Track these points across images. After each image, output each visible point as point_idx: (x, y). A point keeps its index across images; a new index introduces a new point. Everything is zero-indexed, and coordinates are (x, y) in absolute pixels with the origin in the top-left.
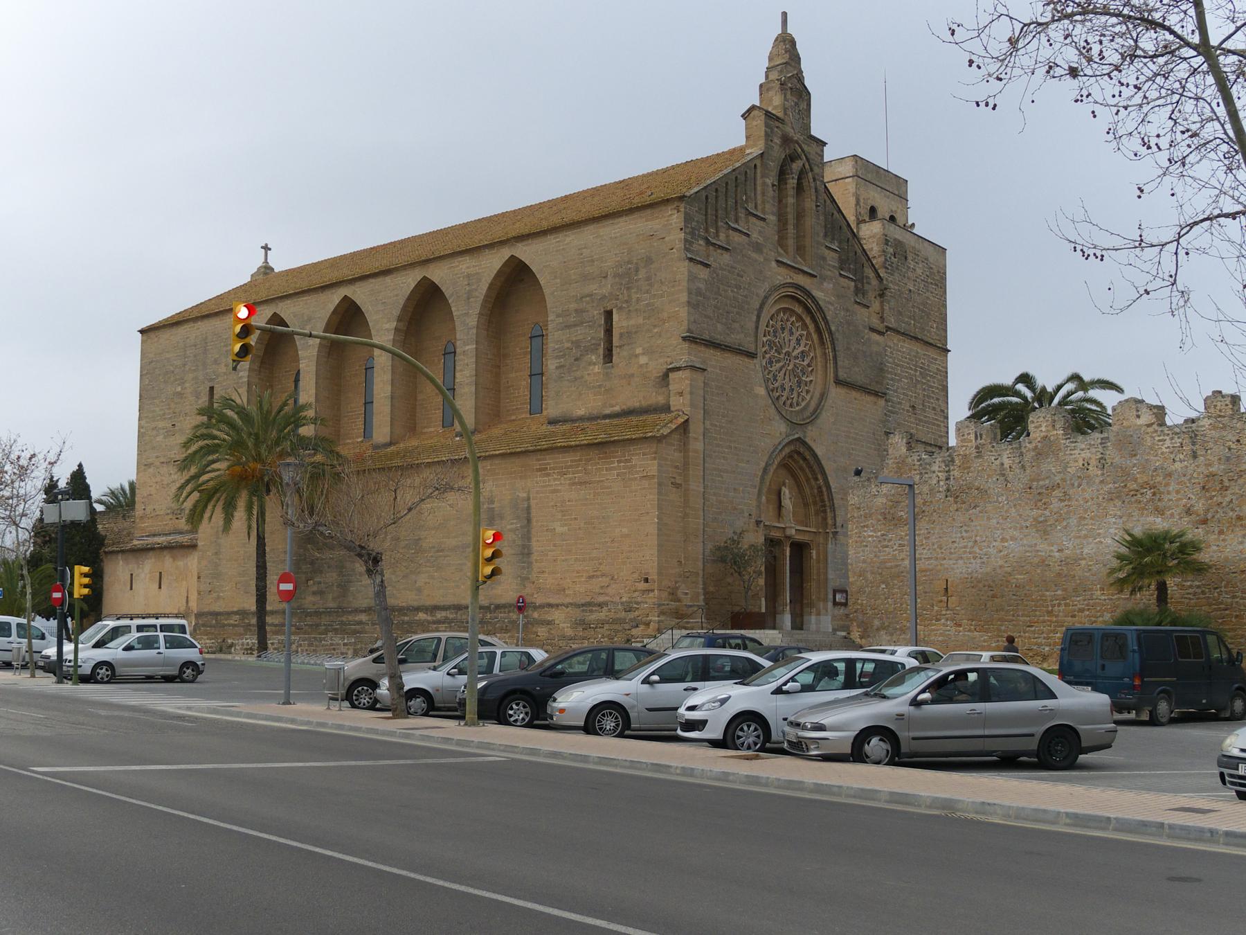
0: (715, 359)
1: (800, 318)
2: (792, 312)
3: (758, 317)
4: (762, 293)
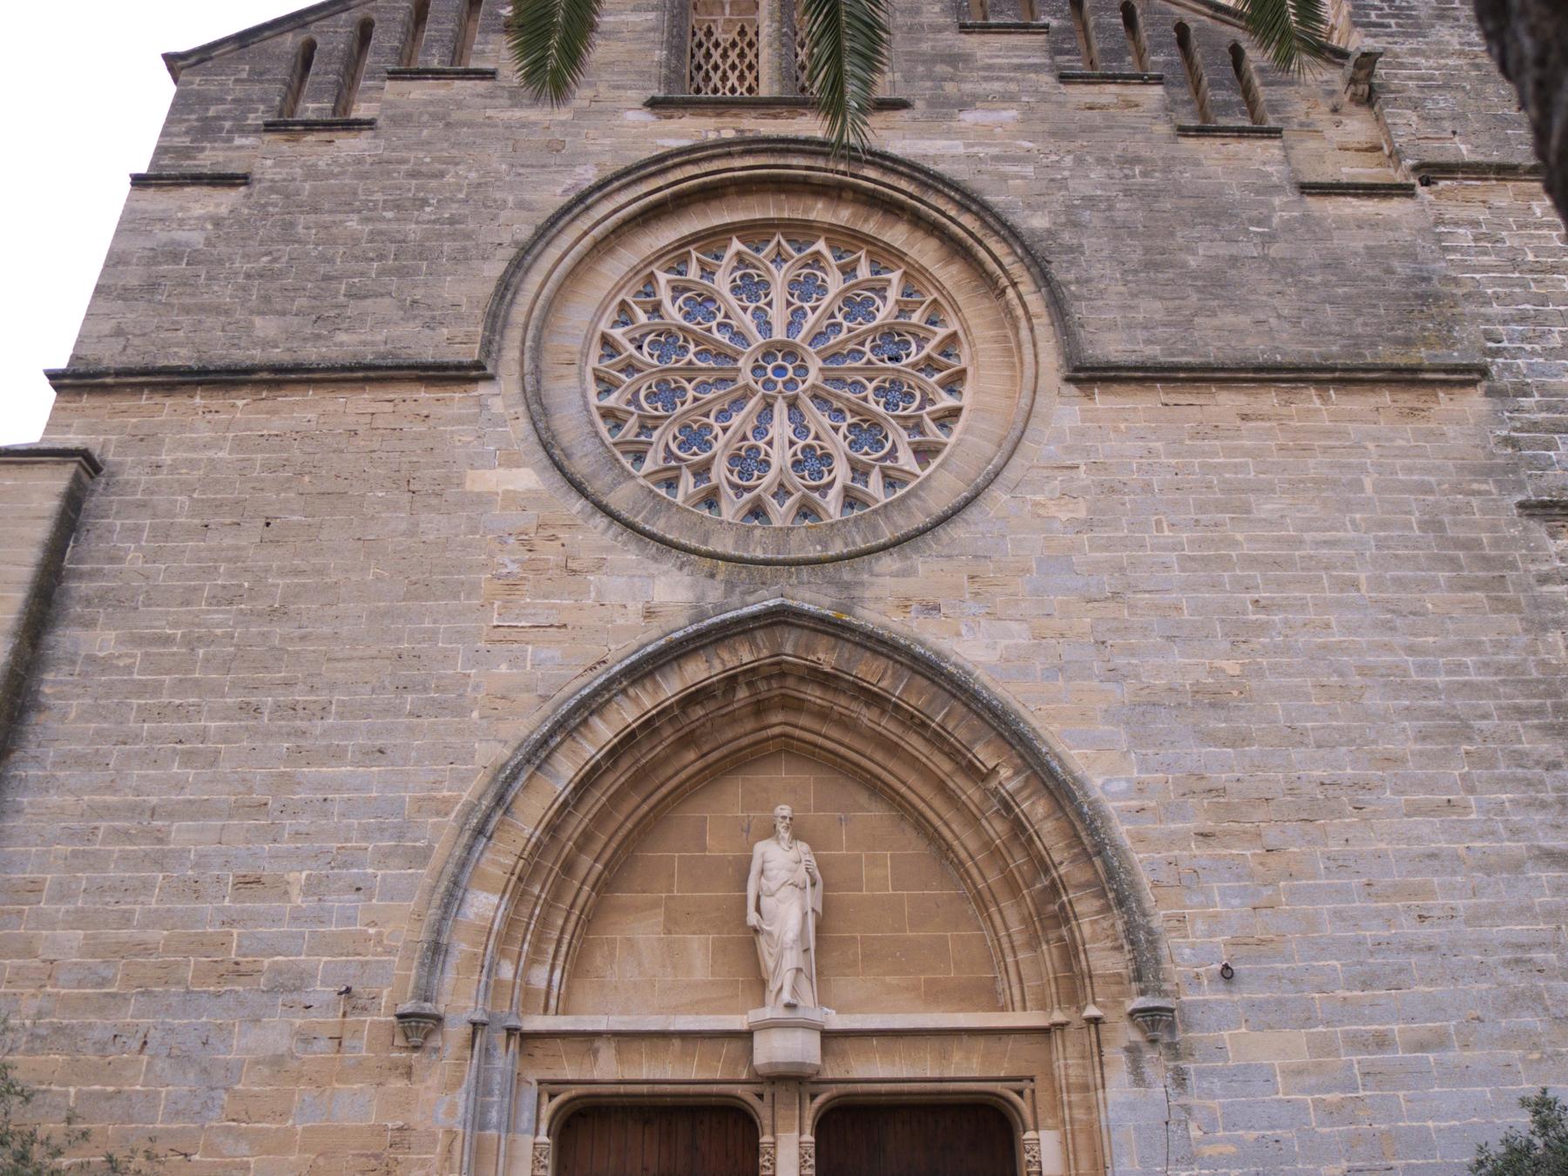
2: (800, 231)
3: (520, 263)
4: (553, 195)
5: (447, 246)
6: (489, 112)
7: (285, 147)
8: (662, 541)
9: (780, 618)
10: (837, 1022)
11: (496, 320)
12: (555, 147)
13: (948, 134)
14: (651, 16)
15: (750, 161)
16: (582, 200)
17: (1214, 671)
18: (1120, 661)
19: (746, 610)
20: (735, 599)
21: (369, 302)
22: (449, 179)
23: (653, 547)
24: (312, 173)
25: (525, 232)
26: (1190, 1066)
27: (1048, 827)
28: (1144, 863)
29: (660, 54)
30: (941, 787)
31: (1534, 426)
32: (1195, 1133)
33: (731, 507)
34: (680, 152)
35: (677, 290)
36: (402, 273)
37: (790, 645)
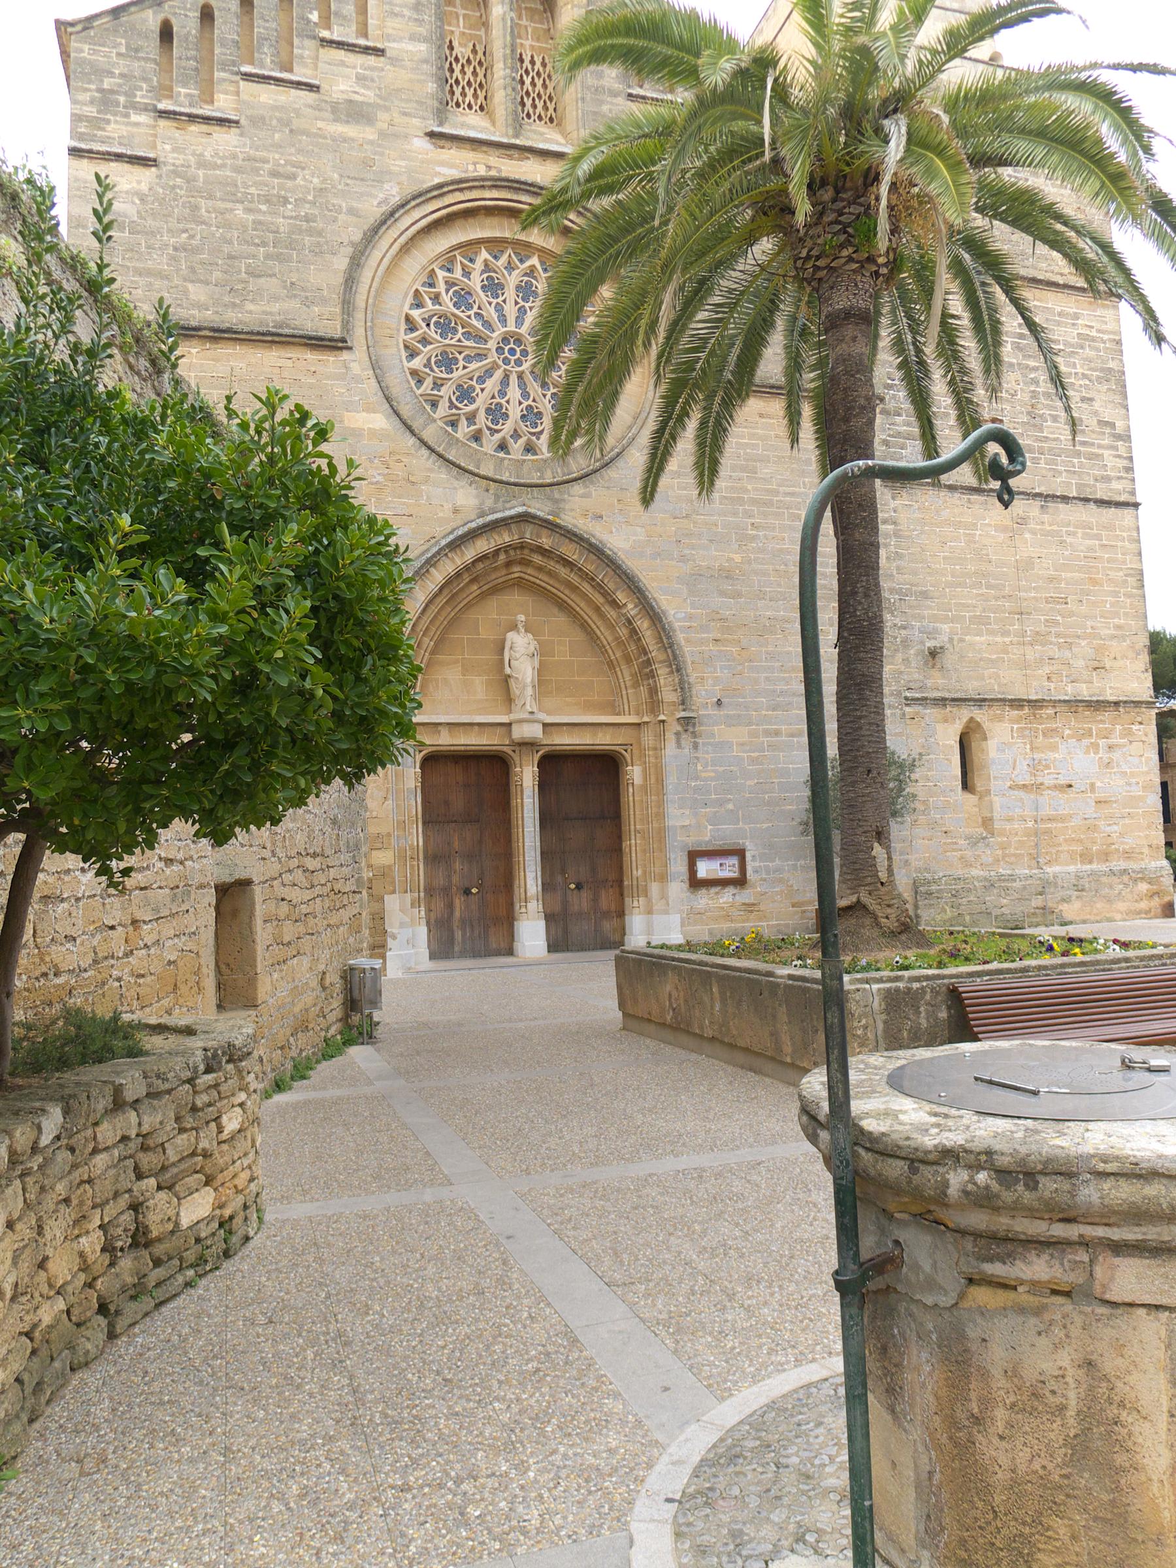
3: (356, 263)
6: (320, 124)
7: (177, 134)
8: (459, 467)
9: (525, 518)
10: (549, 719)
11: (347, 305)
12: (367, 164)
14: (423, 47)
15: (495, 194)
16: (391, 215)
17: (730, 560)
18: (687, 552)
19: (508, 513)
20: (500, 505)
21: (262, 280)
22: (299, 181)
23: (455, 470)
24: (202, 164)
26: (700, 741)
27: (648, 633)
28: (688, 652)
29: (431, 87)
30: (597, 609)
31: (899, 434)
32: (699, 768)
33: (489, 443)
34: (453, 182)
35: (450, 284)
36: (279, 258)
37: (529, 533)
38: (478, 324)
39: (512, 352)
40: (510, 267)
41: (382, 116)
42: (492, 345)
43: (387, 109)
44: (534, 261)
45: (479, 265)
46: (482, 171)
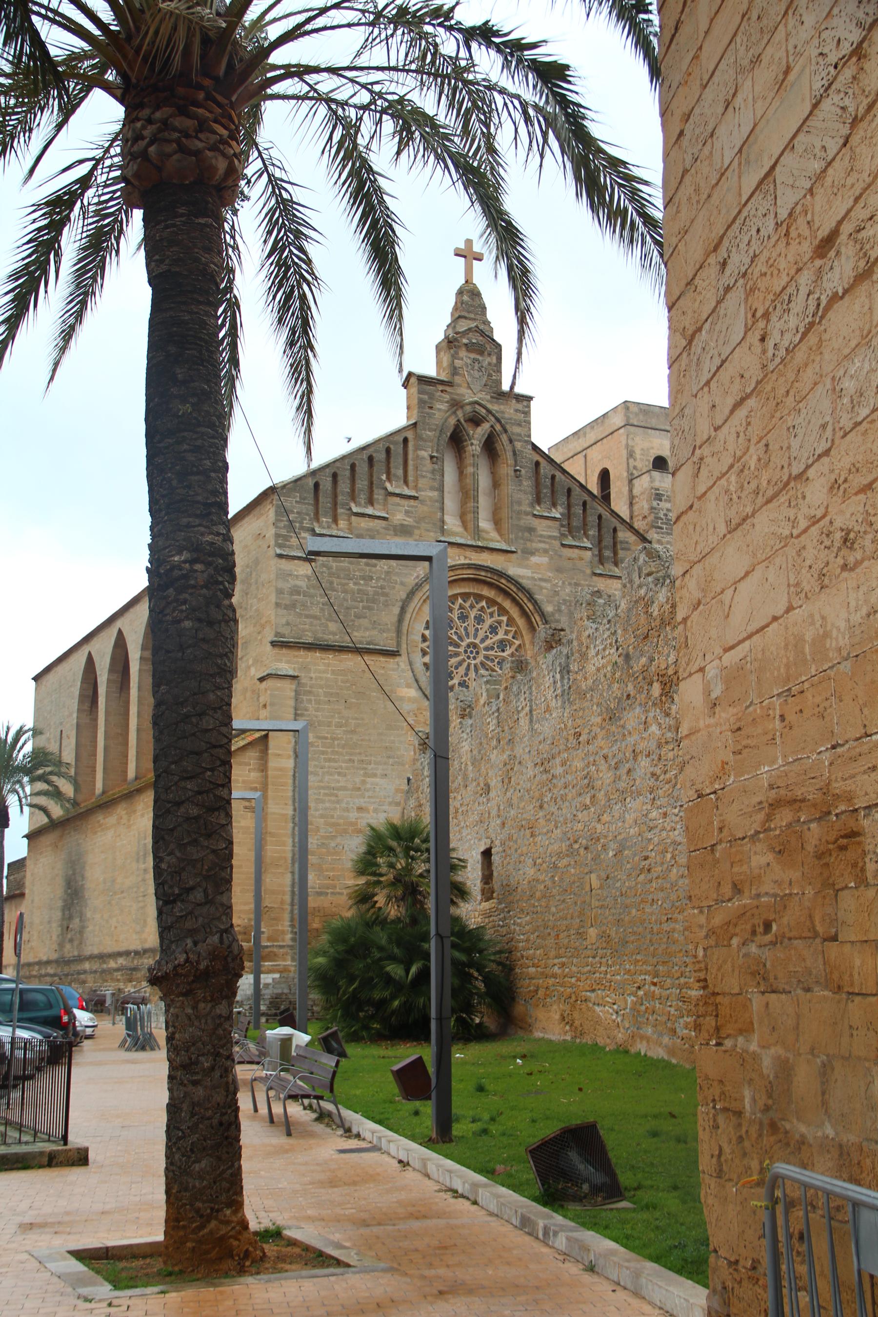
0: (321, 668)
1: (491, 602)
2: (479, 597)
3: (403, 610)
5: (382, 599)
11: (399, 631)
13: (527, 567)
14: (436, 493)
15: (469, 572)
25: (403, 595)
36: (369, 608)
38: (455, 637)
39: (472, 652)
40: (472, 607)
41: (417, 532)
42: (461, 650)
43: (419, 528)
44: (484, 603)
45: (456, 607)
46: (463, 561)
